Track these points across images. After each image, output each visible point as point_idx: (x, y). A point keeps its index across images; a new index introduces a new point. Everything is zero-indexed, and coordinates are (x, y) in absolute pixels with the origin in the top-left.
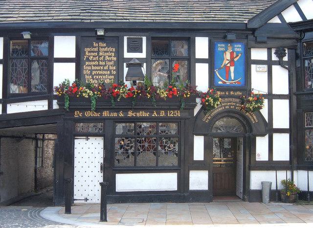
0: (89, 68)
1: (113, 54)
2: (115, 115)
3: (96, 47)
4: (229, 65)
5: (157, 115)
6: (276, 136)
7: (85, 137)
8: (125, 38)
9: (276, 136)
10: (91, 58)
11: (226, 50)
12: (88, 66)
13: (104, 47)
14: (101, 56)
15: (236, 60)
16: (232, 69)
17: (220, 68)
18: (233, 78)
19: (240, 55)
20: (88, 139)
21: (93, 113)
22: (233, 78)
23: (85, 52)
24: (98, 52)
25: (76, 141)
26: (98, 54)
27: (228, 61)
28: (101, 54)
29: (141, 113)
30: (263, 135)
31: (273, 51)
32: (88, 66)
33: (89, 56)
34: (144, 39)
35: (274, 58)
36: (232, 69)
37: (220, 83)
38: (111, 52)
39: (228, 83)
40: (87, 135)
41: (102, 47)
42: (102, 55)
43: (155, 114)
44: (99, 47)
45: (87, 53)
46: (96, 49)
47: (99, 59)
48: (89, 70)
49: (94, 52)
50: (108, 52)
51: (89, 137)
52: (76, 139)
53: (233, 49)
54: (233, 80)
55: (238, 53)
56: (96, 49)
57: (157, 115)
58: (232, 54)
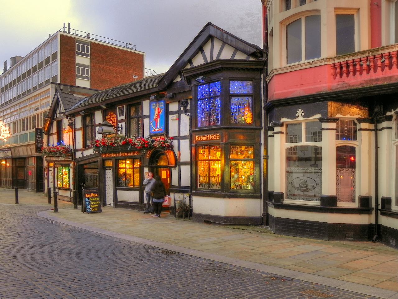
4: (157, 118)
15: (160, 113)
19: (162, 109)
24: (110, 118)
26: (111, 119)
27: (157, 115)
35: (182, 108)
36: (159, 120)
37: (153, 131)
41: (112, 115)
55: (161, 108)
58: (158, 109)
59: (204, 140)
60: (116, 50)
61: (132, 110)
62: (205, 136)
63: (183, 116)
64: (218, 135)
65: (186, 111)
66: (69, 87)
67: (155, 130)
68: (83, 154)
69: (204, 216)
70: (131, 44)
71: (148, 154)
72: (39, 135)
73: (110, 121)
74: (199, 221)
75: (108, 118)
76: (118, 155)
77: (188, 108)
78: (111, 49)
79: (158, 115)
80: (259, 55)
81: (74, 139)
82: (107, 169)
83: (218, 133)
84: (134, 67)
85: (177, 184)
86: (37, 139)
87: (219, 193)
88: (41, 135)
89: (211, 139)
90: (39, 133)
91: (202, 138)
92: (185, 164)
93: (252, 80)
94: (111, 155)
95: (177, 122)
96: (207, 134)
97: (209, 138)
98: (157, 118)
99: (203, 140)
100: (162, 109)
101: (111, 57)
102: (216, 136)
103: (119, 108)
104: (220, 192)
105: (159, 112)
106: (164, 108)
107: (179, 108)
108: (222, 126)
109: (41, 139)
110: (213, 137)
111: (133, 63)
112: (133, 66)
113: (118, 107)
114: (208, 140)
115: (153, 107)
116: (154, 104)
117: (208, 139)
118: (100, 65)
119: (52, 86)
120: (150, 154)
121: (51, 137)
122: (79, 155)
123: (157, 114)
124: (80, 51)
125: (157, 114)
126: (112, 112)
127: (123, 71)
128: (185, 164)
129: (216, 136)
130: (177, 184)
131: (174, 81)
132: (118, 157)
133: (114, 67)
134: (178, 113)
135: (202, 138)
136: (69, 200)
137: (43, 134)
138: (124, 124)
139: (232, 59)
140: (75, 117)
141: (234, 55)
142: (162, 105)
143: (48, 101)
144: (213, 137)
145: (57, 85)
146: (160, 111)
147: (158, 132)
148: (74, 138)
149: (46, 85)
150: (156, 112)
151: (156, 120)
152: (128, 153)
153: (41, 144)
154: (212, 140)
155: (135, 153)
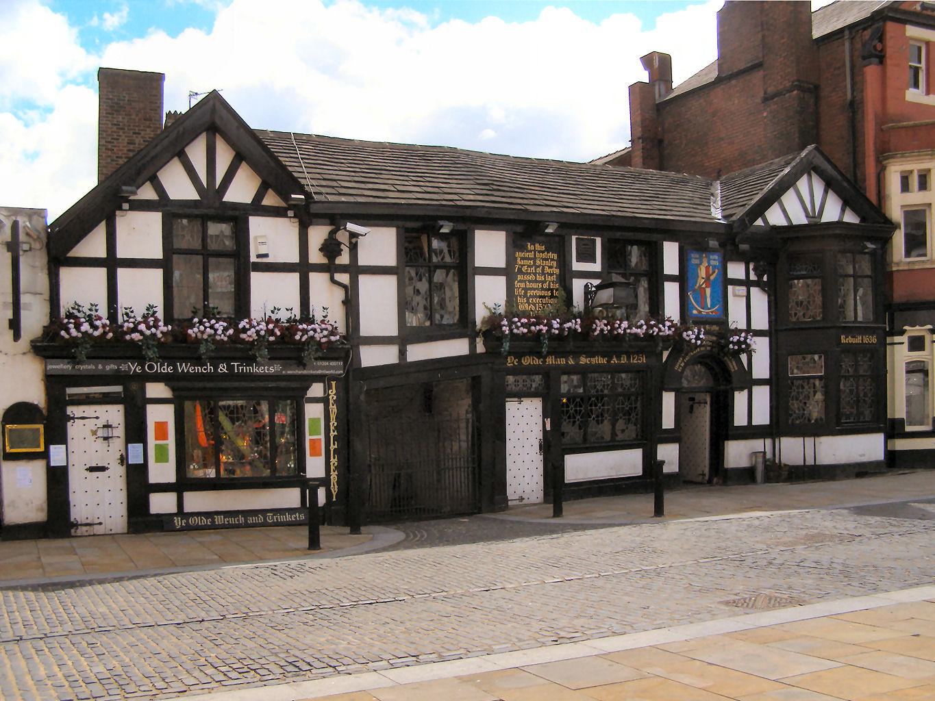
0: (523, 285)
2: (562, 361)
3: (531, 251)
4: (704, 286)
6: (756, 389)
7: (516, 399)
8: (574, 238)
9: (756, 389)
12: (521, 281)
13: (543, 252)
14: (539, 267)
15: (712, 278)
16: (708, 291)
21: (533, 359)
23: (516, 259)
24: (534, 259)
26: (535, 262)
28: (538, 262)
29: (597, 358)
30: (741, 389)
31: (751, 266)
33: (522, 266)
34: (598, 241)
35: (753, 277)
36: (708, 291)
37: (695, 312)
38: (552, 260)
39: (704, 312)
40: (520, 395)
41: (539, 252)
43: (615, 359)
44: (535, 251)
45: (518, 261)
46: (531, 255)
47: (535, 270)
48: (523, 289)
49: (529, 259)
50: (547, 260)
51: (522, 399)
52: (507, 401)
53: (709, 262)
54: (709, 309)
55: (714, 267)
56: (531, 255)
58: (707, 268)
65: (757, 284)
67: (700, 312)
68: (402, 353)
71: (680, 361)
74: (847, 477)
75: (522, 259)
76: (571, 362)
77: (765, 278)
81: (351, 304)
82: (507, 399)
85: (745, 423)
91: (850, 340)
92: (761, 382)
96: (859, 334)
105: (708, 276)
108: (875, 323)
113: (574, 238)
115: (694, 262)
122: (371, 357)
123: (703, 278)
125: (703, 278)
128: (761, 382)
130: (745, 423)
135: (850, 340)
146: (711, 272)
150: (703, 273)
152: (610, 358)
155: (634, 359)
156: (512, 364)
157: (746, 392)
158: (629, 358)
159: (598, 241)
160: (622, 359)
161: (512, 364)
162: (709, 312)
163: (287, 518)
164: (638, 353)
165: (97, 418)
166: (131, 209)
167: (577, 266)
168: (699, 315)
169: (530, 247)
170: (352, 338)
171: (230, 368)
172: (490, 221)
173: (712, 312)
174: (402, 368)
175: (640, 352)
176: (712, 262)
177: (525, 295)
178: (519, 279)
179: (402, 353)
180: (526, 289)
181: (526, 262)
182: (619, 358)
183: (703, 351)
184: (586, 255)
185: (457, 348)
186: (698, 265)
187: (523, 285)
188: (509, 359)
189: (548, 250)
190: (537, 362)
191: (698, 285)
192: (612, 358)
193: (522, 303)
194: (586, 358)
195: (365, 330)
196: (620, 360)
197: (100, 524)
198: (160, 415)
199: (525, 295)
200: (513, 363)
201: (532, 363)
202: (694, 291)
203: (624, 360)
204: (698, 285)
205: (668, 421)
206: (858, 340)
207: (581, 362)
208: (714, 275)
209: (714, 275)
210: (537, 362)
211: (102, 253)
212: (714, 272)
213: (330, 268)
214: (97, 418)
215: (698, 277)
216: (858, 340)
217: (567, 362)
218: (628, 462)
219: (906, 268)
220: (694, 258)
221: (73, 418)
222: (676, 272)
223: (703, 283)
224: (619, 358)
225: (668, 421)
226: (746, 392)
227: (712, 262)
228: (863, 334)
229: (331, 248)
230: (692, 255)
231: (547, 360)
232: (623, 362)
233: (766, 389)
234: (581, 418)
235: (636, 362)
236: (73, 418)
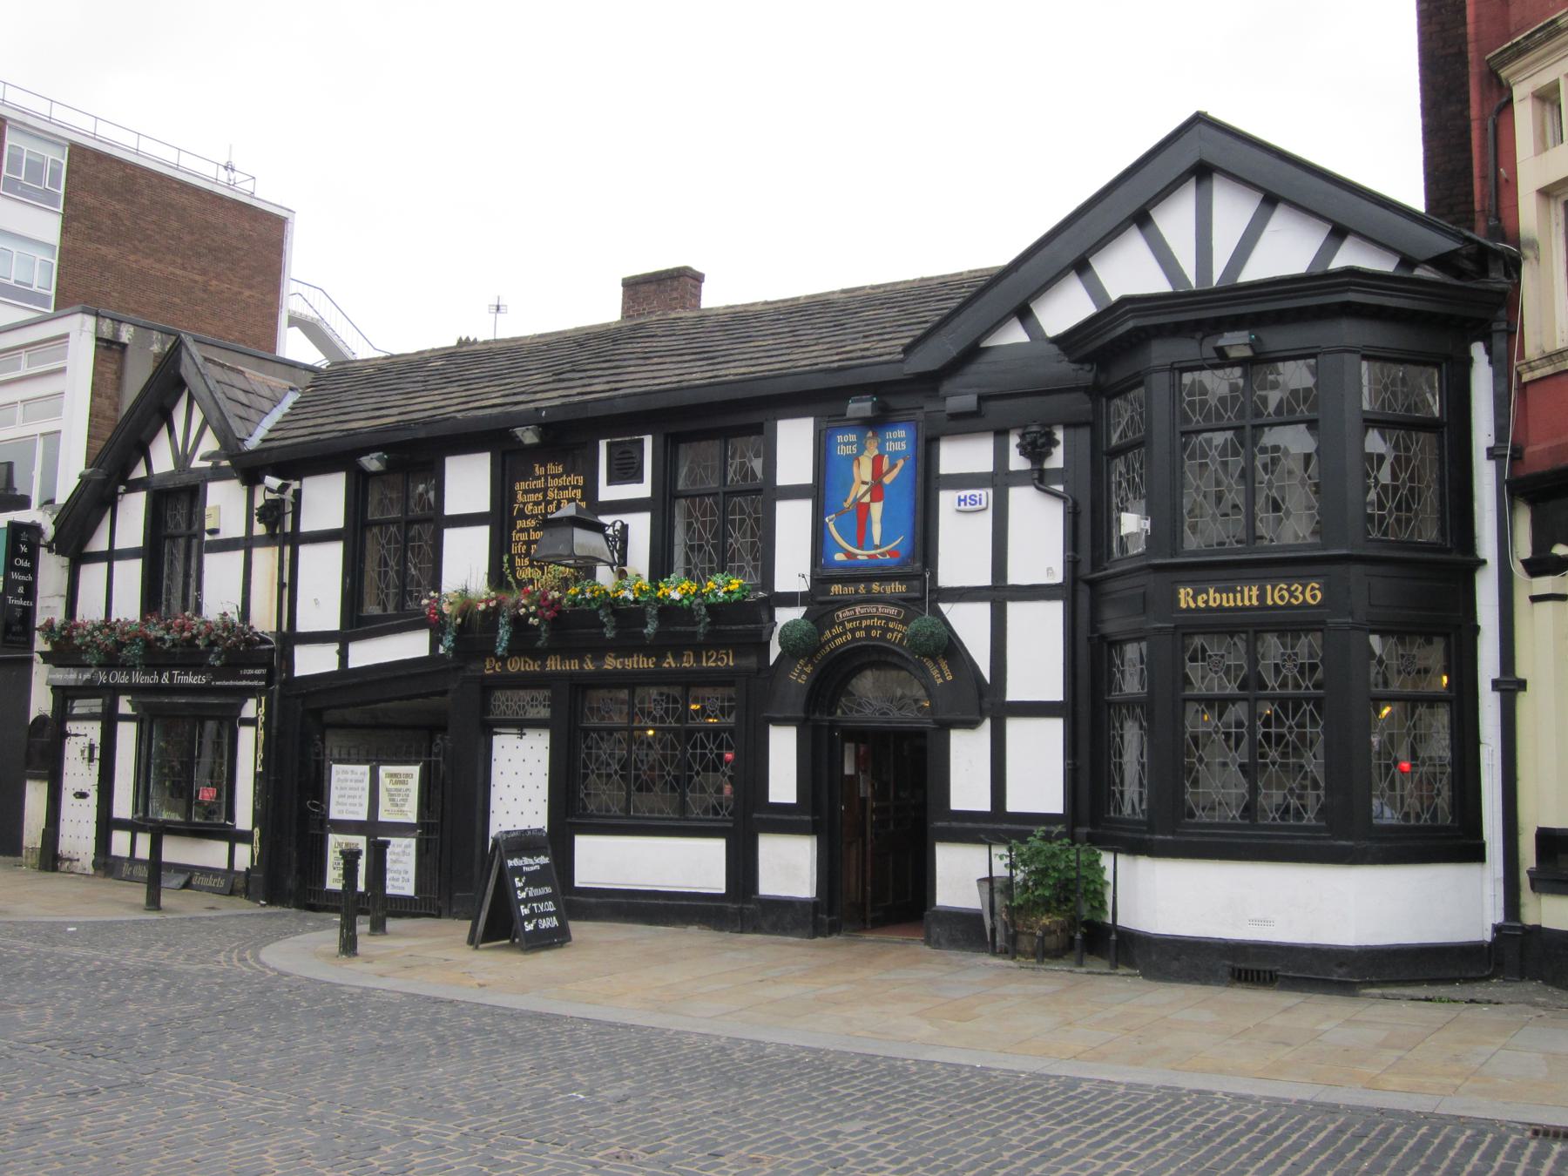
0: (524, 537)
1: (579, 493)
2: (574, 665)
3: (539, 478)
4: (867, 499)
5: (673, 665)
6: (1016, 728)
7: (515, 731)
9: (1016, 728)
10: (528, 509)
11: (862, 449)
12: (522, 530)
13: (559, 476)
14: (551, 502)
15: (887, 480)
16: (876, 510)
17: (841, 512)
18: (877, 540)
19: (901, 463)
20: (522, 735)
21: (525, 662)
22: (877, 540)
24: (545, 490)
25: (498, 741)
26: (545, 496)
27: (865, 487)
28: (551, 495)
29: (635, 659)
30: (971, 724)
31: (1014, 440)
32: (522, 530)
33: (525, 504)
34: (648, 441)
35: (1017, 462)
36: (876, 510)
37: (839, 557)
38: (575, 487)
39: (862, 555)
40: (521, 725)
41: (553, 477)
42: (554, 499)
43: (670, 660)
44: (546, 476)
45: (519, 497)
46: (540, 484)
47: (546, 508)
48: (525, 542)
49: (535, 491)
51: (525, 731)
52: (500, 734)
53: (881, 447)
54: (877, 547)
55: (894, 456)
56: (540, 484)
57: (673, 665)
58: (877, 461)
59: (1229, 609)
60: (175, 189)
61: (681, 463)
62: (1235, 592)
63: (1022, 499)
64: (1281, 589)
65: (1040, 479)
66: (156, 335)
67: (848, 554)
68: (343, 656)
69: (1001, 952)
70: (233, 170)
72: (24, 556)
73: (537, 504)
75: (526, 492)
76: (589, 666)
77: (1057, 460)
78: (155, 181)
79: (877, 491)
80: (1468, 265)
81: (288, 587)
82: (495, 730)
83: (1313, 577)
84: (244, 268)
85: (984, 805)
86: (15, 576)
87: (1322, 842)
88: (33, 557)
89: (1270, 602)
90: (24, 549)
91: (1215, 598)
93: (1437, 365)
94: (543, 666)
95: (986, 520)
97: (1262, 596)
98: (867, 499)
99: (1220, 608)
100: (901, 463)
101: (154, 218)
102: (1303, 593)
103: (609, 446)
104: (1324, 838)
105: (877, 473)
106: (916, 459)
107: (1001, 456)
109: (30, 578)
110: (1282, 597)
111: (242, 253)
112: (243, 264)
113: (603, 445)
114: (1251, 608)
116: (853, 438)
117: (1255, 602)
118: (104, 250)
119: (83, 325)
120: (813, 665)
121: (93, 576)
122: (312, 661)
123: (864, 483)
124: (22, 178)
125: (864, 483)
126: (555, 461)
127: (196, 282)
129: (1303, 593)
130: (984, 805)
131: (984, 344)
132: (590, 674)
133: (160, 261)
134: (999, 481)
135: (1215, 598)
136: (220, 883)
137: (43, 551)
138: (640, 527)
139: (1319, 270)
140: (301, 480)
141: (1326, 252)
142: (899, 440)
143: (59, 390)
144: (1282, 597)
145: (108, 321)
147: (874, 561)
148: (286, 579)
149: (61, 312)
150: (864, 471)
151: (863, 511)
152: (661, 657)
153: (25, 603)
154: (1275, 607)
155: (708, 659)
156: (491, 671)
157: (984, 732)
158: (698, 658)
159: (648, 441)
160: (685, 659)
161: (491, 671)
162: (874, 556)
163: (209, 882)
164: (717, 647)
165: (86, 735)
166: (127, 492)
167: (608, 492)
168: (852, 561)
169: (539, 470)
170: (290, 638)
171: (171, 677)
172: (465, 440)
173: (883, 554)
174: (345, 680)
175: (716, 641)
176: (891, 447)
177: (528, 553)
178: (518, 527)
179: (343, 656)
180: (529, 543)
181: (533, 497)
182: (678, 656)
183: (860, 639)
184: (625, 470)
185: (412, 646)
186: (855, 458)
187: (524, 537)
188: (487, 663)
189: (567, 473)
190: (533, 667)
191: (850, 499)
192: (665, 657)
193: (521, 567)
194: (616, 658)
195: (302, 626)
196: (682, 662)
197: (78, 860)
198: (127, 734)
199: (528, 553)
200: (494, 668)
201: (523, 669)
202: (841, 512)
203: (688, 662)
204: (850, 499)
205: (783, 785)
206: (1248, 596)
207: (606, 667)
208: (896, 472)
209: (896, 472)
210: (533, 667)
211: (105, 547)
212: (893, 466)
213: (270, 539)
214: (86, 735)
215: (853, 481)
216: (1248, 596)
217: (581, 668)
218: (123, 807)
219: (1548, 370)
220: (845, 443)
221: (70, 735)
222: (806, 477)
223: (864, 495)
224: (678, 656)
225: (783, 785)
226: (984, 732)
227: (891, 447)
228: (1261, 581)
229: (272, 513)
230: (840, 438)
231: (548, 662)
232: (687, 665)
233: (1052, 731)
234: (621, 769)
235: (714, 665)
236: (70, 735)
